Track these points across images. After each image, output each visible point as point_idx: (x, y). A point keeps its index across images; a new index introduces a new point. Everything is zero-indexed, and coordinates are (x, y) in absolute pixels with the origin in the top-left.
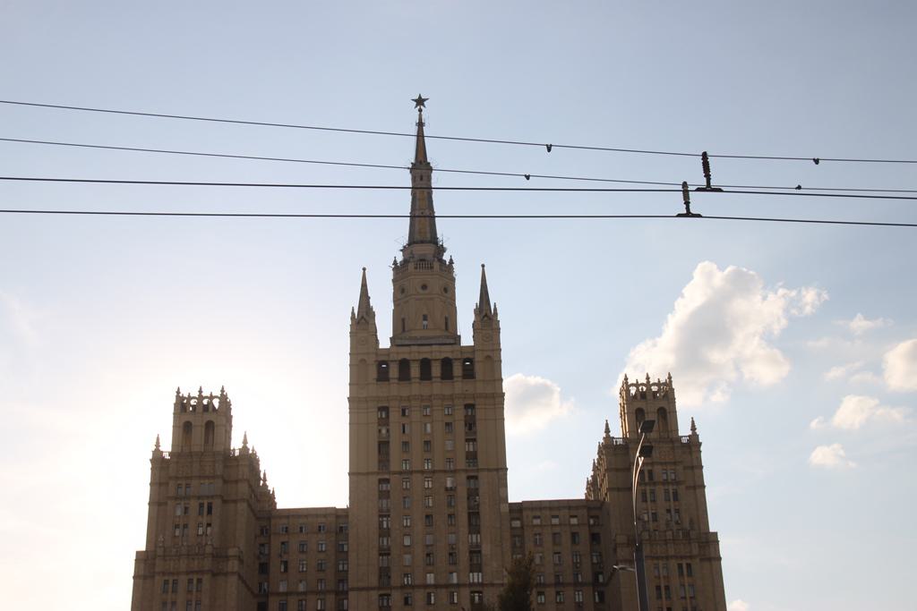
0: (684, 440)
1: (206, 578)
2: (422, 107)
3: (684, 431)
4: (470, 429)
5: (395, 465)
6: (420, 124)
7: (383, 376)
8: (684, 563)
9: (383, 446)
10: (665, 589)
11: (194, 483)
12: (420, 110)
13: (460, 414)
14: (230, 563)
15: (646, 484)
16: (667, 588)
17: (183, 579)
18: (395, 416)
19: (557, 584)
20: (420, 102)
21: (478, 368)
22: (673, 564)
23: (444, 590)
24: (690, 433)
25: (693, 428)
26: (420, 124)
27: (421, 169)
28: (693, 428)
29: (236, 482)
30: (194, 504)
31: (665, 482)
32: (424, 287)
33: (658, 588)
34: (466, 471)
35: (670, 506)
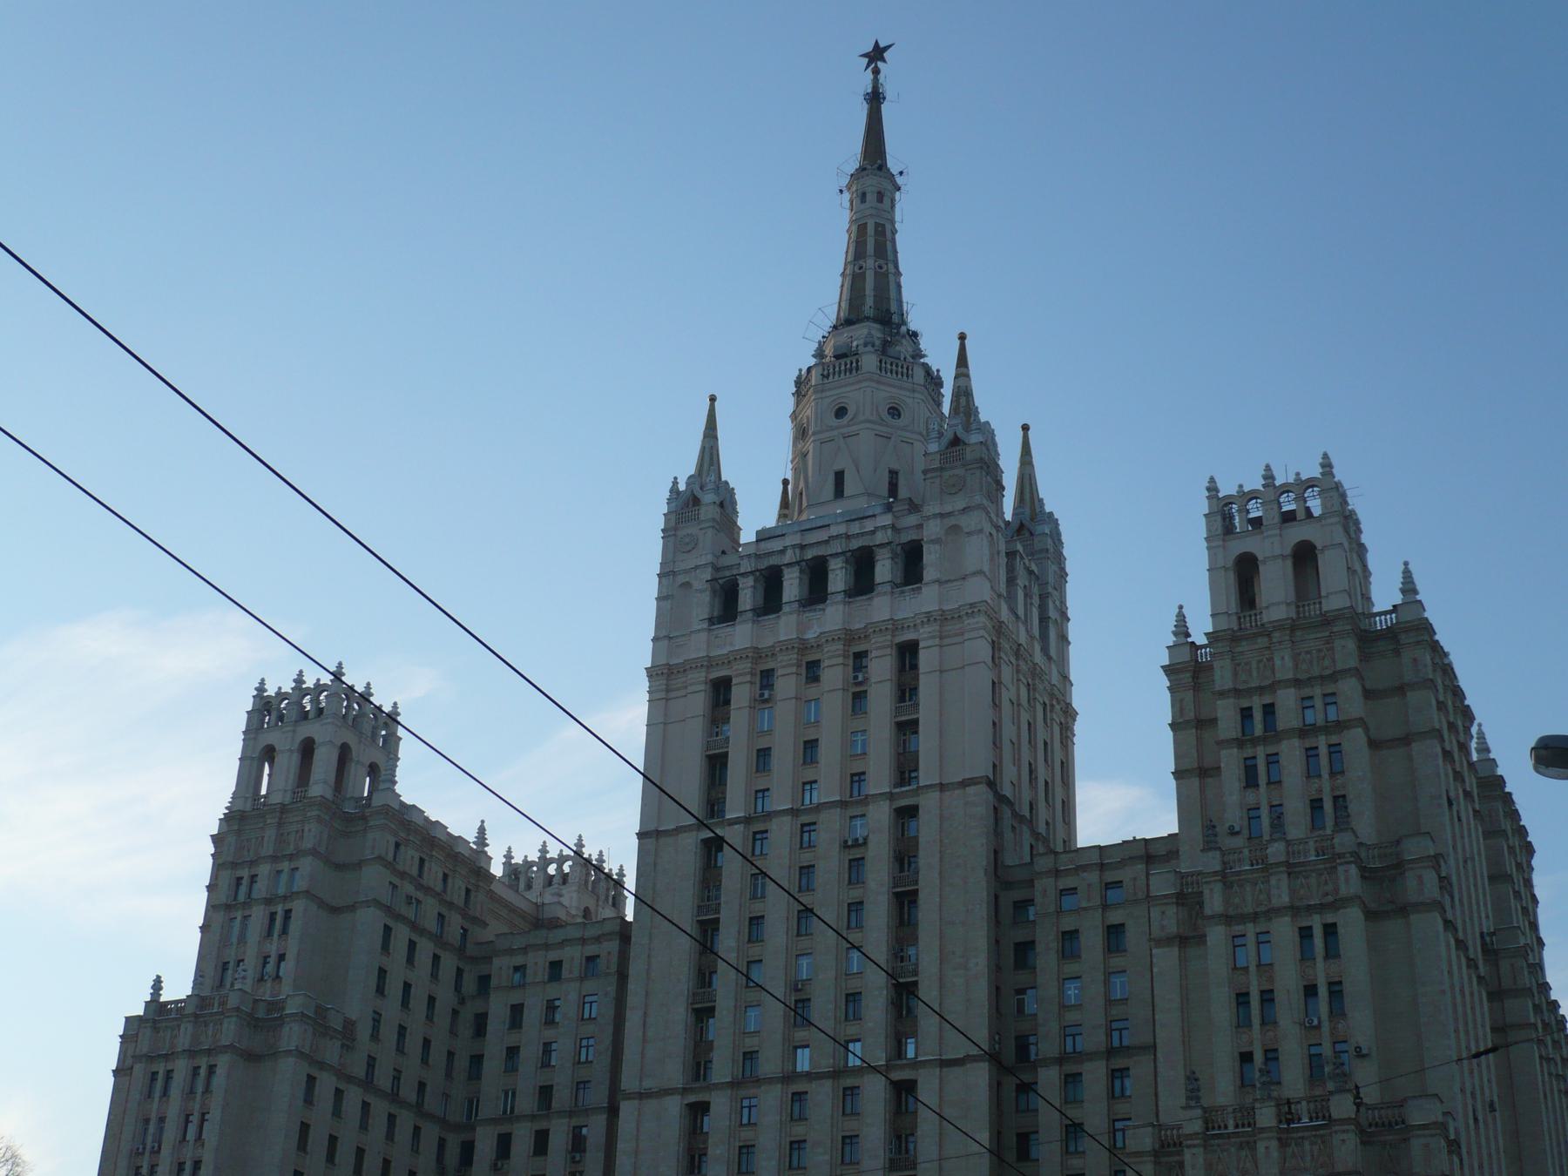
0: (1381, 624)
1: (223, 1062)
2: (880, 64)
3: (1384, 595)
4: (902, 699)
5: (735, 807)
6: (875, 98)
7: (727, 608)
8: (1316, 923)
9: (716, 765)
10: (1263, 1001)
11: (264, 870)
12: (876, 72)
13: (882, 668)
14: (286, 1029)
15: (1255, 742)
16: (1267, 997)
17: (181, 1067)
18: (741, 695)
19: (1111, 1052)
20: (876, 55)
21: (930, 556)
22: (1284, 930)
23: (828, 1083)
24: (1398, 599)
25: (1409, 587)
26: (875, 98)
27: (874, 178)
28: (1409, 587)
29: (359, 865)
30: (258, 914)
31: (1305, 732)
32: (841, 412)
33: (1242, 999)
34: (891, 796)
35: (1320, 791)
